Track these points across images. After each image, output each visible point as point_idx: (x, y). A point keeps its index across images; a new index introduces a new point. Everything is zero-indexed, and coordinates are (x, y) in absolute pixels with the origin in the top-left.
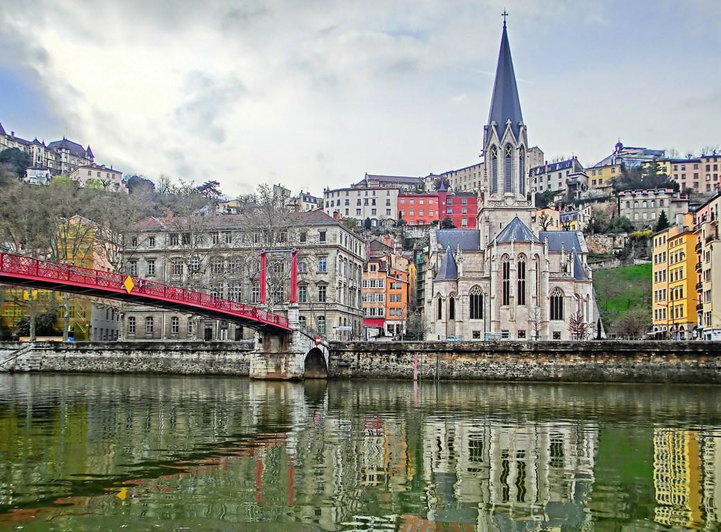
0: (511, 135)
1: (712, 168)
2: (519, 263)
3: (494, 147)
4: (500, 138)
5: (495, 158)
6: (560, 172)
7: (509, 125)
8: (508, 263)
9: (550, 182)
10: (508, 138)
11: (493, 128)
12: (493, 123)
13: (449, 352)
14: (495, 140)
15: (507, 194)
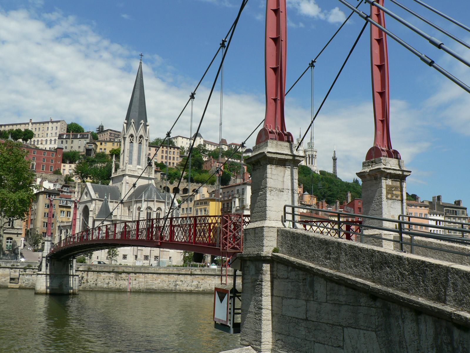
0: (143, 130)
1: (164, 152)
2: (147, 213)
3: (132, 136)
4: (137, 129)
5: (132, 142)
6: (80, 139)
7: (142, 124)
8: (150, 213)
9: (72, 145)
10: (141, 132)
11: (132, 123)
12: (133, 121)
13: (151, 273)
14: (132, 131)
15: (139, 167)
